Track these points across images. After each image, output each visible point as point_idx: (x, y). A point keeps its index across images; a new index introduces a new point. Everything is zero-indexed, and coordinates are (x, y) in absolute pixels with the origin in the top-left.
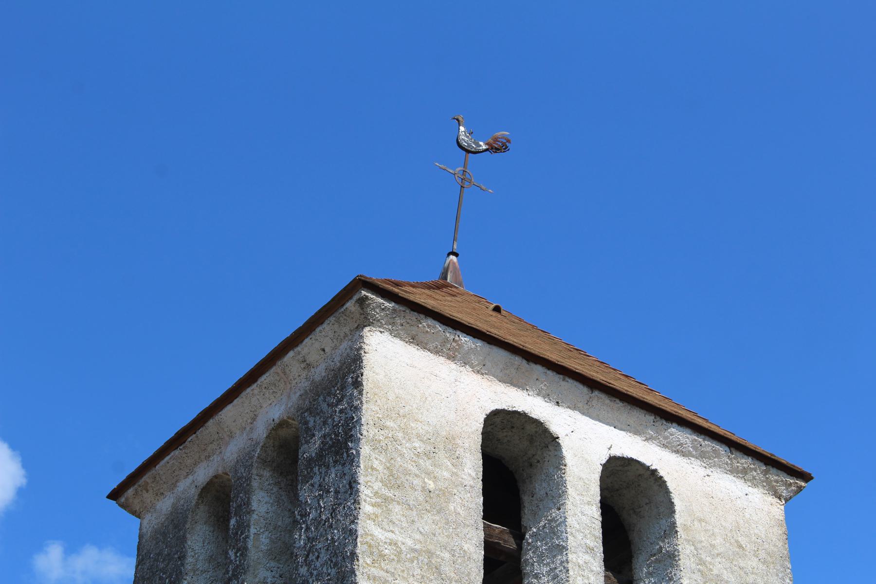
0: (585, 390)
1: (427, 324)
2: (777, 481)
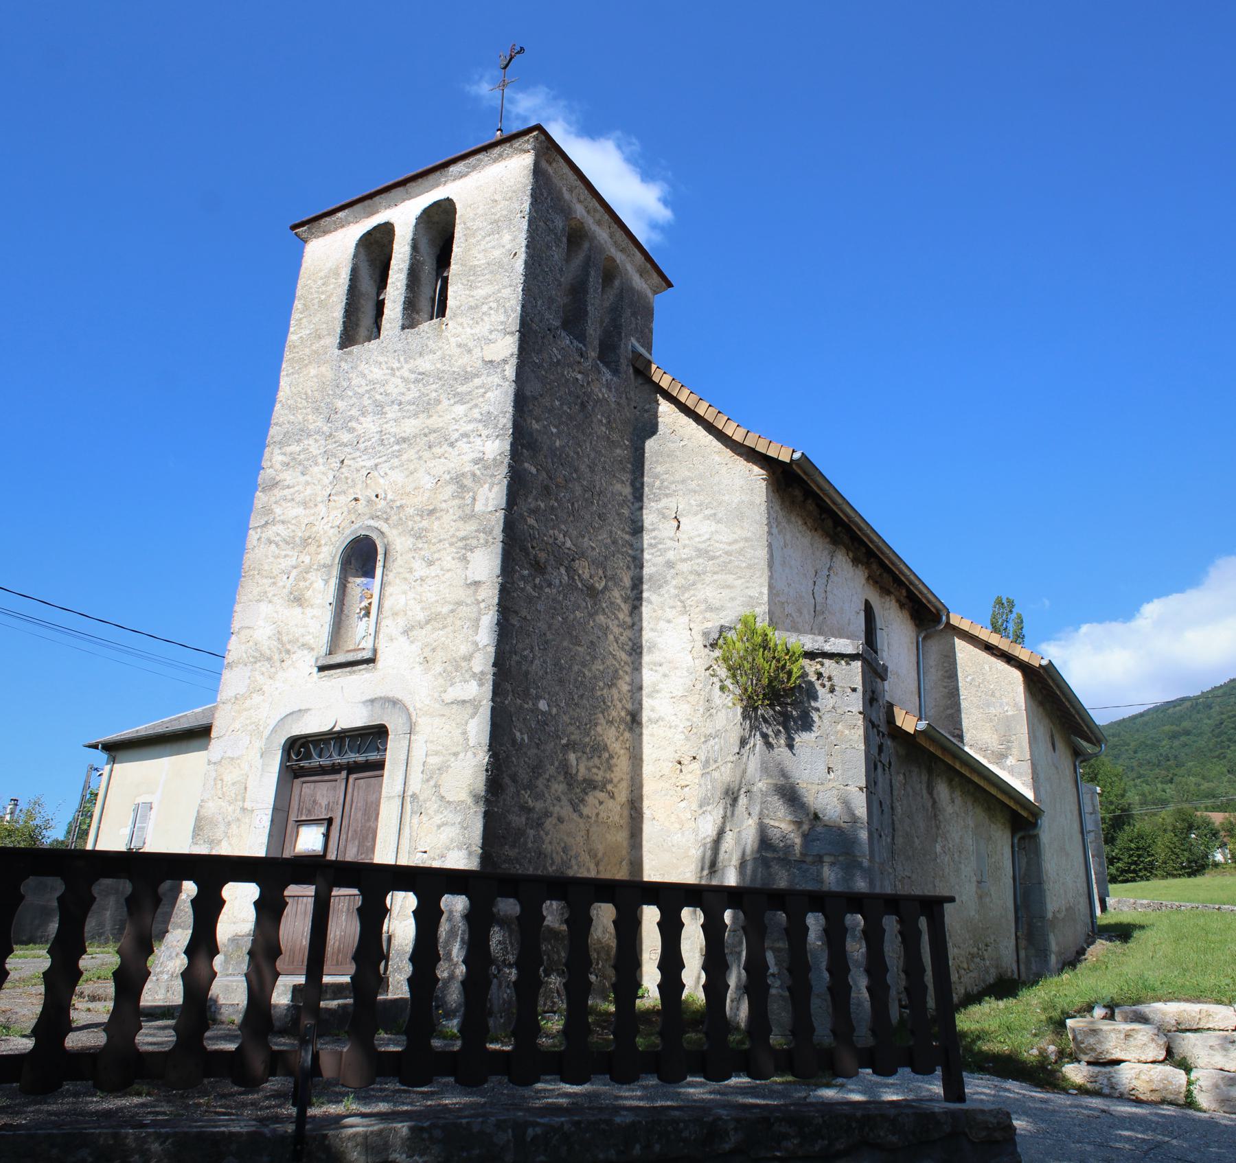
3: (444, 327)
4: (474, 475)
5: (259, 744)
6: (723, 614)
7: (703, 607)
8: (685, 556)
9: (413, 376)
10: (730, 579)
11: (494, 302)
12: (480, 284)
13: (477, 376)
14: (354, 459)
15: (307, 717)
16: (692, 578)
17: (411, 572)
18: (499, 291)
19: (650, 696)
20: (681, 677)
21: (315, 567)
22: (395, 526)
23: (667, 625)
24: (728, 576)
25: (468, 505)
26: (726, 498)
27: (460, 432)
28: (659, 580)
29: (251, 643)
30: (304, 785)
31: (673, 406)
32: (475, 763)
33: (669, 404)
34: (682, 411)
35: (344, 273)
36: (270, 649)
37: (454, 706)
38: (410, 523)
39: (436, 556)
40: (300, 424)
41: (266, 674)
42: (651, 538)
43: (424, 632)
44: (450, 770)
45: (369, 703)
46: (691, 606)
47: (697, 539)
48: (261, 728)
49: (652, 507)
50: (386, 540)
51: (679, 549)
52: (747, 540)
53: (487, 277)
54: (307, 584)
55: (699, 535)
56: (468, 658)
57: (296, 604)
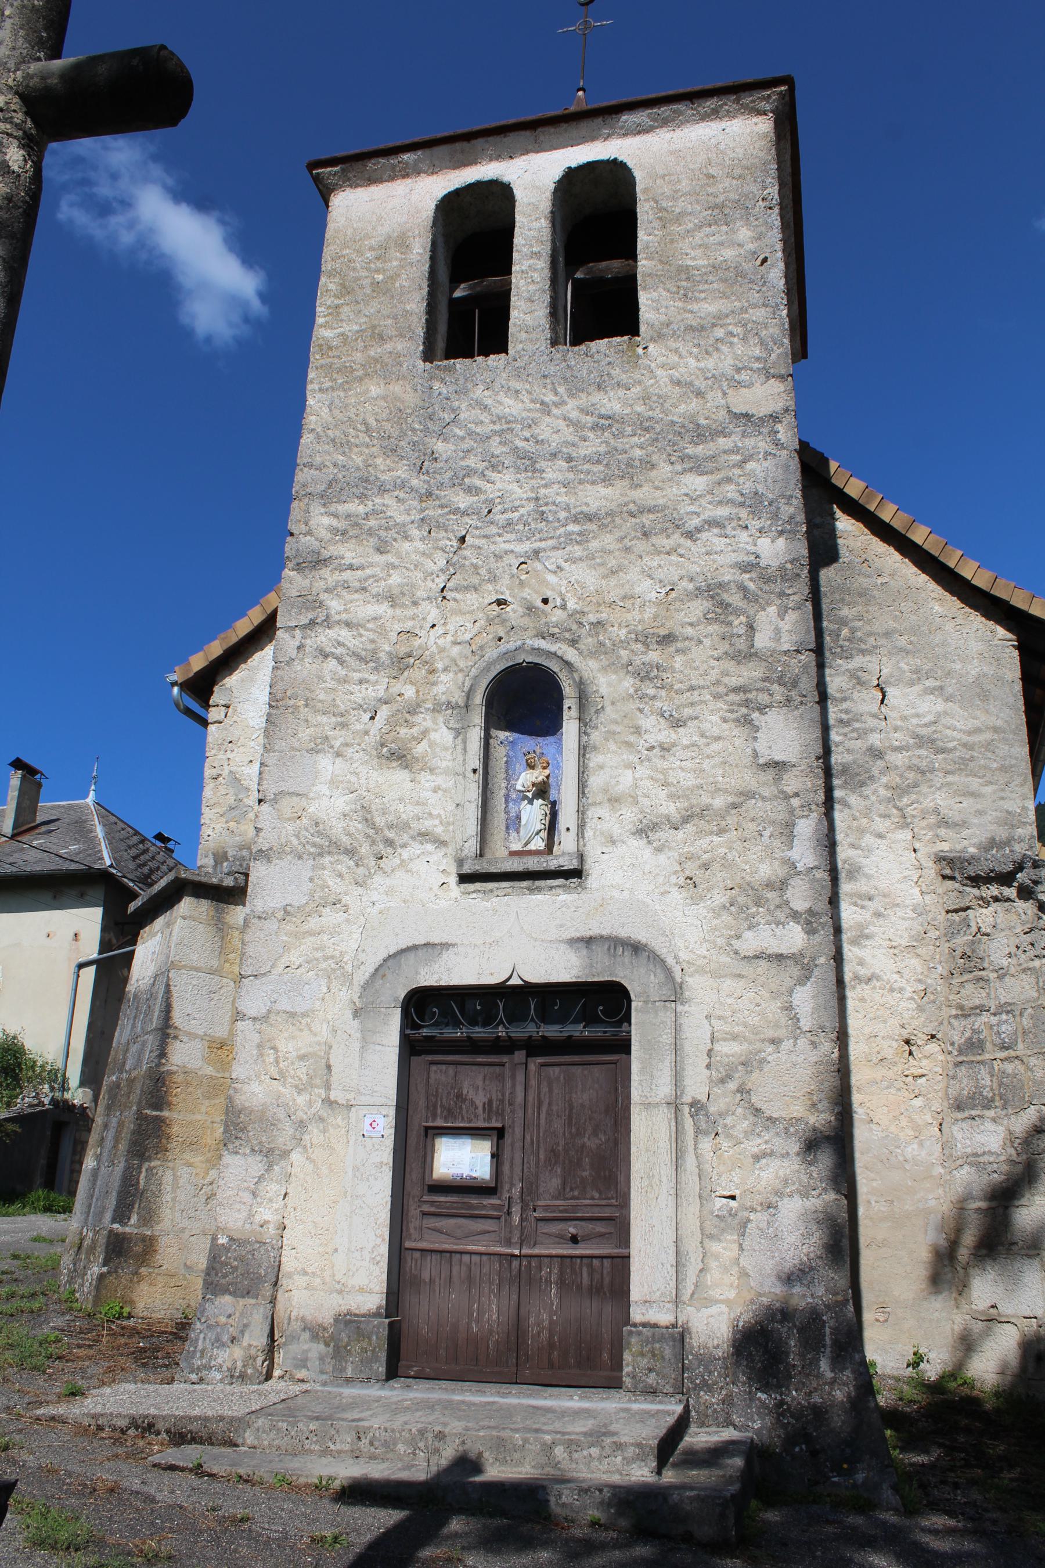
0: (528, 133)
1: (371, 165)
2: (753, 101)
3: (640, 351)
4: (743, 589)
5: (345, 996)
6: (966, 833)
7: (932, 819)
8: (897, 744)
9: (590, 420)
10: (974, 783)
11: (736, 325)
12: (703, 295)
13: (723, 433)
14: (485, 537)
15: (448, 956)
16: (911, 776)
17: (640, 734)
18: (744, 310)
19: (854, 942)
20: (904, 919)
21: (429, 705)
22: (593, 654)
23: (879, 841)
24: (970, 779)
25: (740, 636)
26: (958, 666)
27: (702, 517)
28: (858, 774)
29: (304, 820)
30: (434, 1068)
31: (862, 526)
32: (814, 1059)
33: (853, 521)
34: (875, 533)
35: (417, 245)
36: (349, 834)
37: (763, 963)
38: (624, 653)
39: (687, 712)
40: (358, 469)
41: (346, 876)
42: (841, 711)
43: (680, 835)
44: (767, 1068)
45: (581, 945)
46: (914, 816)
47: (915, 721)
48: (349, 968)
49: (839, 666)
50: (576, 675)
51: (887, 733)
52: (996, 730)
53: (715, 285)
54: (415, 731)
55: (918, 716)
56: (782, 885)
57: (394, 764)
